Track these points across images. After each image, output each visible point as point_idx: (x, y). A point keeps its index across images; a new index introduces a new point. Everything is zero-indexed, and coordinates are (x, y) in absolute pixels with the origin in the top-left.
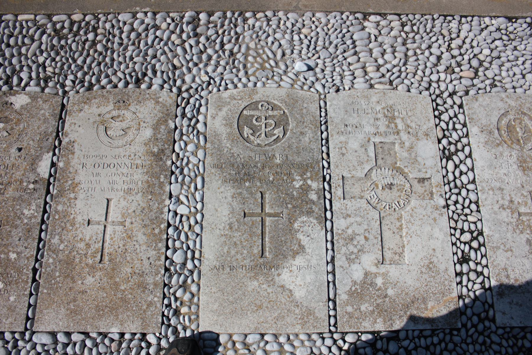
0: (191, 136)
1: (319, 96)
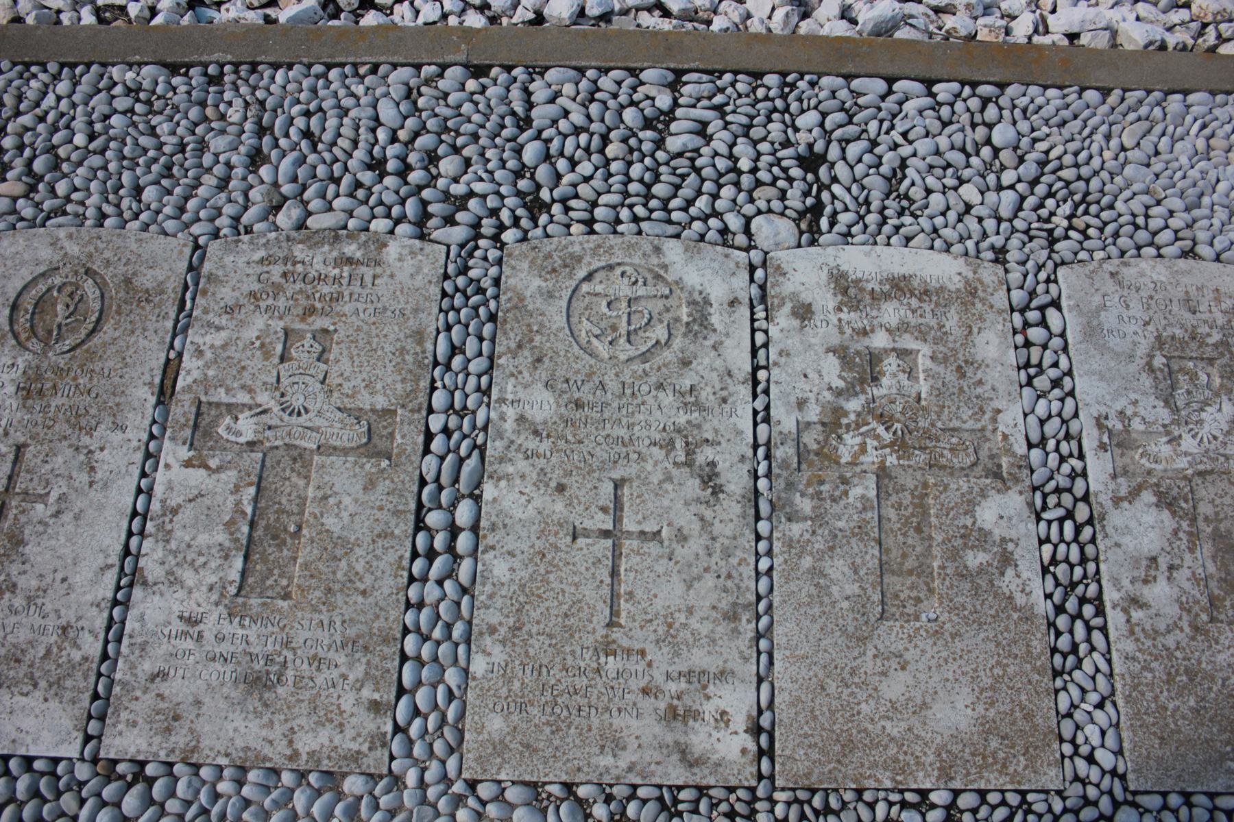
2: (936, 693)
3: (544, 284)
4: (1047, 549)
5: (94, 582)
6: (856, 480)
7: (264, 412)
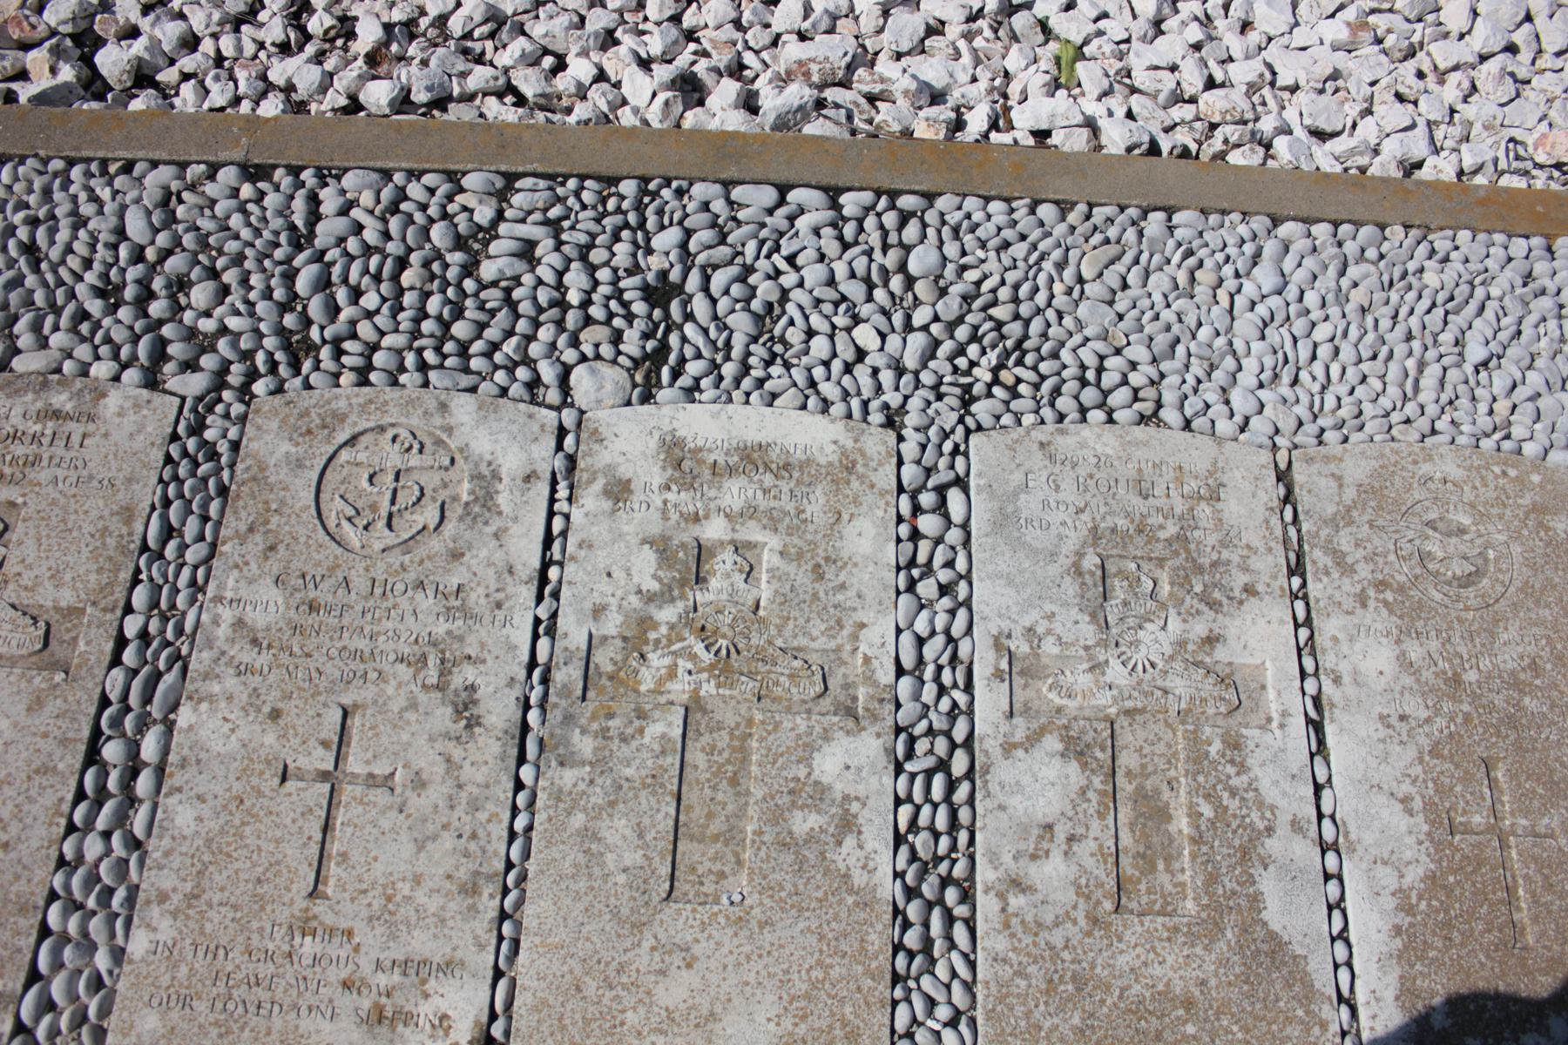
2: (729, 1000)
3: (293, 450)
4: (905, 812)
6: (657, 714)
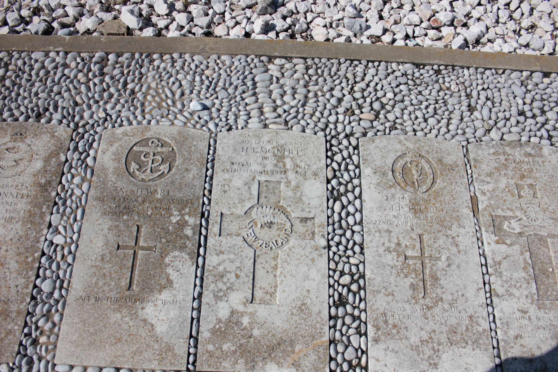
0: (79, 170)
1: (210, 134)
5: (476, 296)
7: (520, 220)
